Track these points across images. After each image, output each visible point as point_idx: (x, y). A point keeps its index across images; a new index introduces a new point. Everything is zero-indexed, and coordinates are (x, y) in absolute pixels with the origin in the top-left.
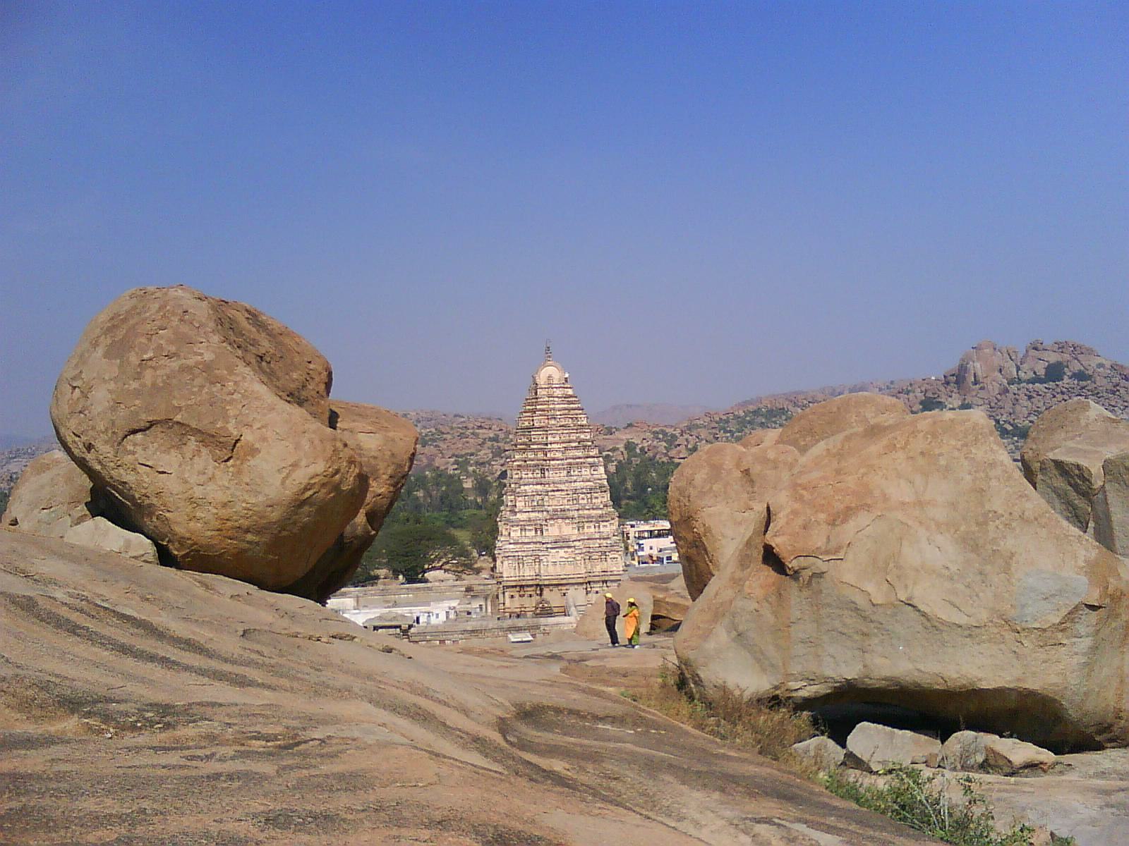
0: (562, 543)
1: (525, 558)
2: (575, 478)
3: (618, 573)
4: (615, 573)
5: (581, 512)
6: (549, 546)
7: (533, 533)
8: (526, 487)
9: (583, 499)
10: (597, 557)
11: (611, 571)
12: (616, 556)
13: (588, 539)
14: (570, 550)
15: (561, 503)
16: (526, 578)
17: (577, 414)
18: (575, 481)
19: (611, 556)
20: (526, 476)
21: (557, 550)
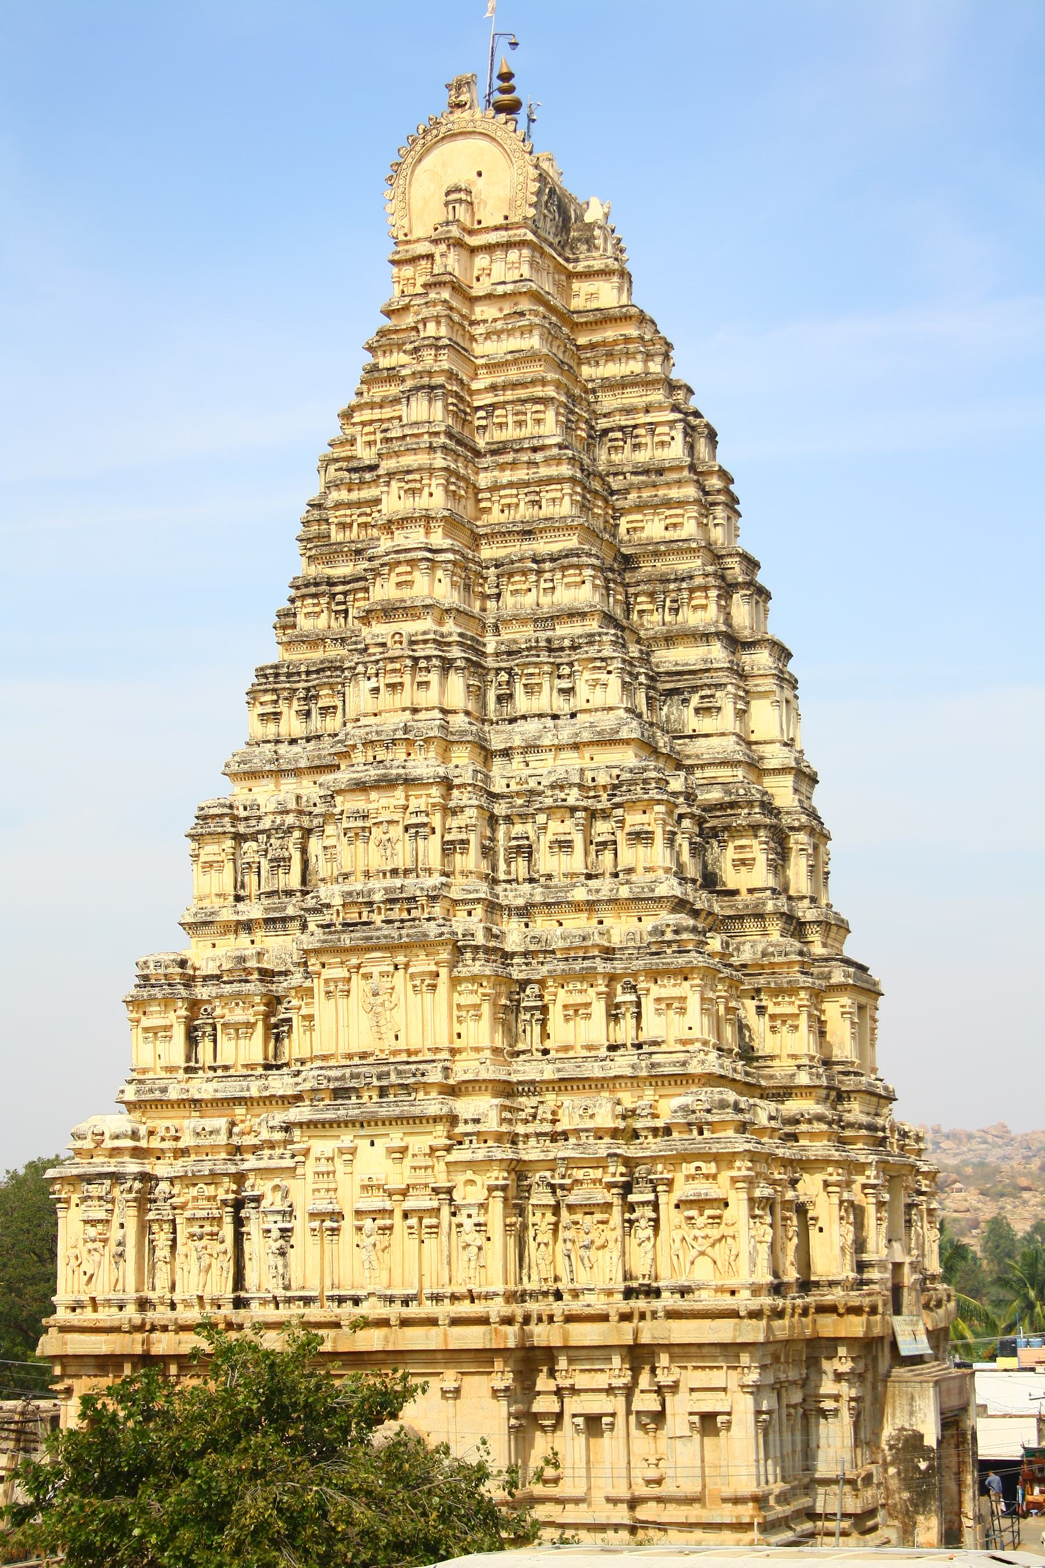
2: (532, 727)
3: (727, 1302)
4: (706, 1300)
9: (564, 845)
10: (602, 1196)
11: (684, 1291)
14: (420, 1143)
15: (402, 861)
17: (628, 411)
18: (531, 748)
19: (683, 1189)
20: (271, 730)
21: (346, 1138)
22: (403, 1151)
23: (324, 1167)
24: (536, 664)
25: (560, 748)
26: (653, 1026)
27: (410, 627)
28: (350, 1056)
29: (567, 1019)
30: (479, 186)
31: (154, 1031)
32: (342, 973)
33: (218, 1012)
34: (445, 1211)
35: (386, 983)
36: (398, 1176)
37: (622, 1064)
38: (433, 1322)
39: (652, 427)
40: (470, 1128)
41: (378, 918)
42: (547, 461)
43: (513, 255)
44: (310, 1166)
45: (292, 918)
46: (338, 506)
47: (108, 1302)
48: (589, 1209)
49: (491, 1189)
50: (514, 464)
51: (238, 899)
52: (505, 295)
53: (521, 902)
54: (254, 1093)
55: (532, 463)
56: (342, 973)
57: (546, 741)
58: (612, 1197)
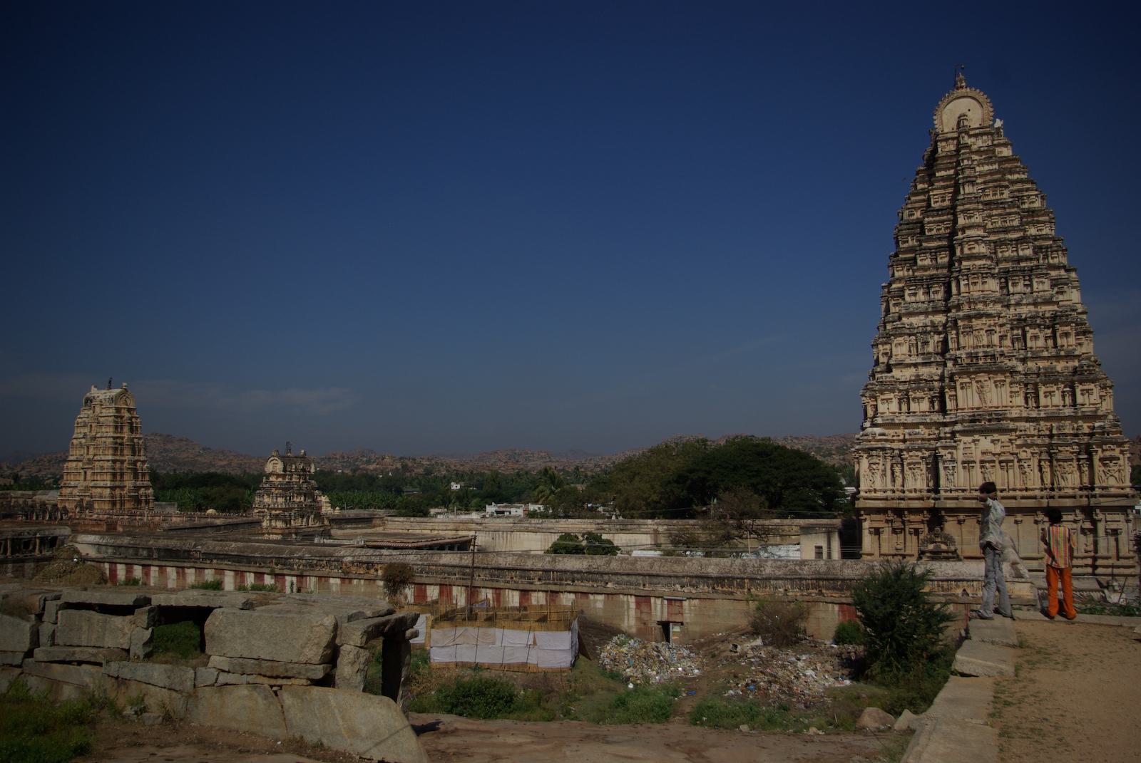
0: (987, 422)
1: (905, 455)
2: (1017, 297)
4: (1113, 491)
5: (1030, 364)
6: (958, 427)
11: (1103, 488)
12: (1117, 453)
13: (1046, 419)
14: (1005, 438)
15: (985, 342)
16: (908, 494)
17: (1019, 191)
18: (1018, 304)
20: (913, 299)
21: (977, 437)
22: (998, 440)
23: (968, 446)
24: (1017, 276)
25: (1028, 304)
26: (1080, 399)
27: (978, 263)
28: (973, 409)
29: (1046, 397)
30: (969, 114)
31: (887, 400)
32: (968, 380)
33: (910, 393)
34: (1016, 460)
35: (986, 383)
36: (998, 449)
37: (1068, 411)
38: (1014, 498)
39: (1029, 196)
40: (1023, 433)
41: (981, 362)
42: (1009, 208)
43: (985, 138)
44: (961, 446)
45: (932, 362)
46: (929, 223)
47: (880, 490)
48: (1065, 461)
49: (1032, 453)
50: (996, 209)
51: (910, 356)
52: (984, 151)
53: (1021, 356)
54: (928, 421)
55: (1005, 208)
56: (968, 380)
57: (1024, 302)
58: (1073, 456)
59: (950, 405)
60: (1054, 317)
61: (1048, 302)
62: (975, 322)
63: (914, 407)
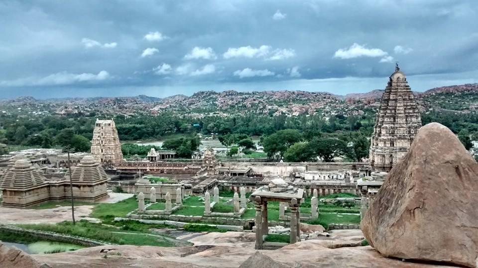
7: (389, 145)
8: (387, 125)
59: (395, 145)
60: (416, 127)
61: (416, 123)
62: (401, 128)
63: (387, 145)
